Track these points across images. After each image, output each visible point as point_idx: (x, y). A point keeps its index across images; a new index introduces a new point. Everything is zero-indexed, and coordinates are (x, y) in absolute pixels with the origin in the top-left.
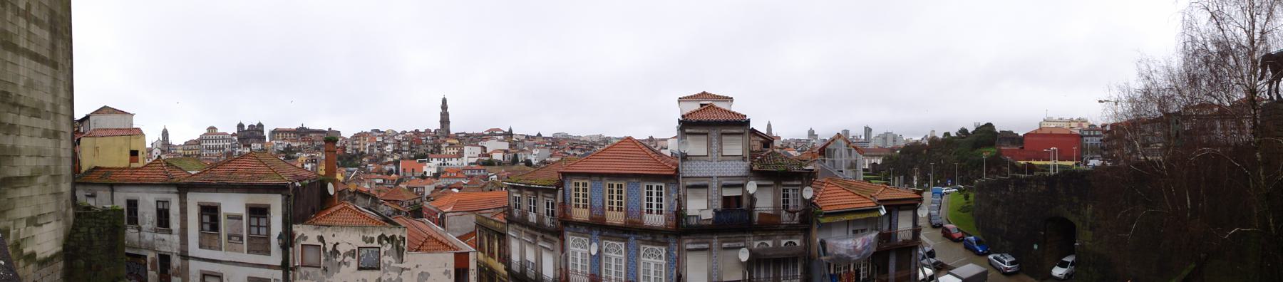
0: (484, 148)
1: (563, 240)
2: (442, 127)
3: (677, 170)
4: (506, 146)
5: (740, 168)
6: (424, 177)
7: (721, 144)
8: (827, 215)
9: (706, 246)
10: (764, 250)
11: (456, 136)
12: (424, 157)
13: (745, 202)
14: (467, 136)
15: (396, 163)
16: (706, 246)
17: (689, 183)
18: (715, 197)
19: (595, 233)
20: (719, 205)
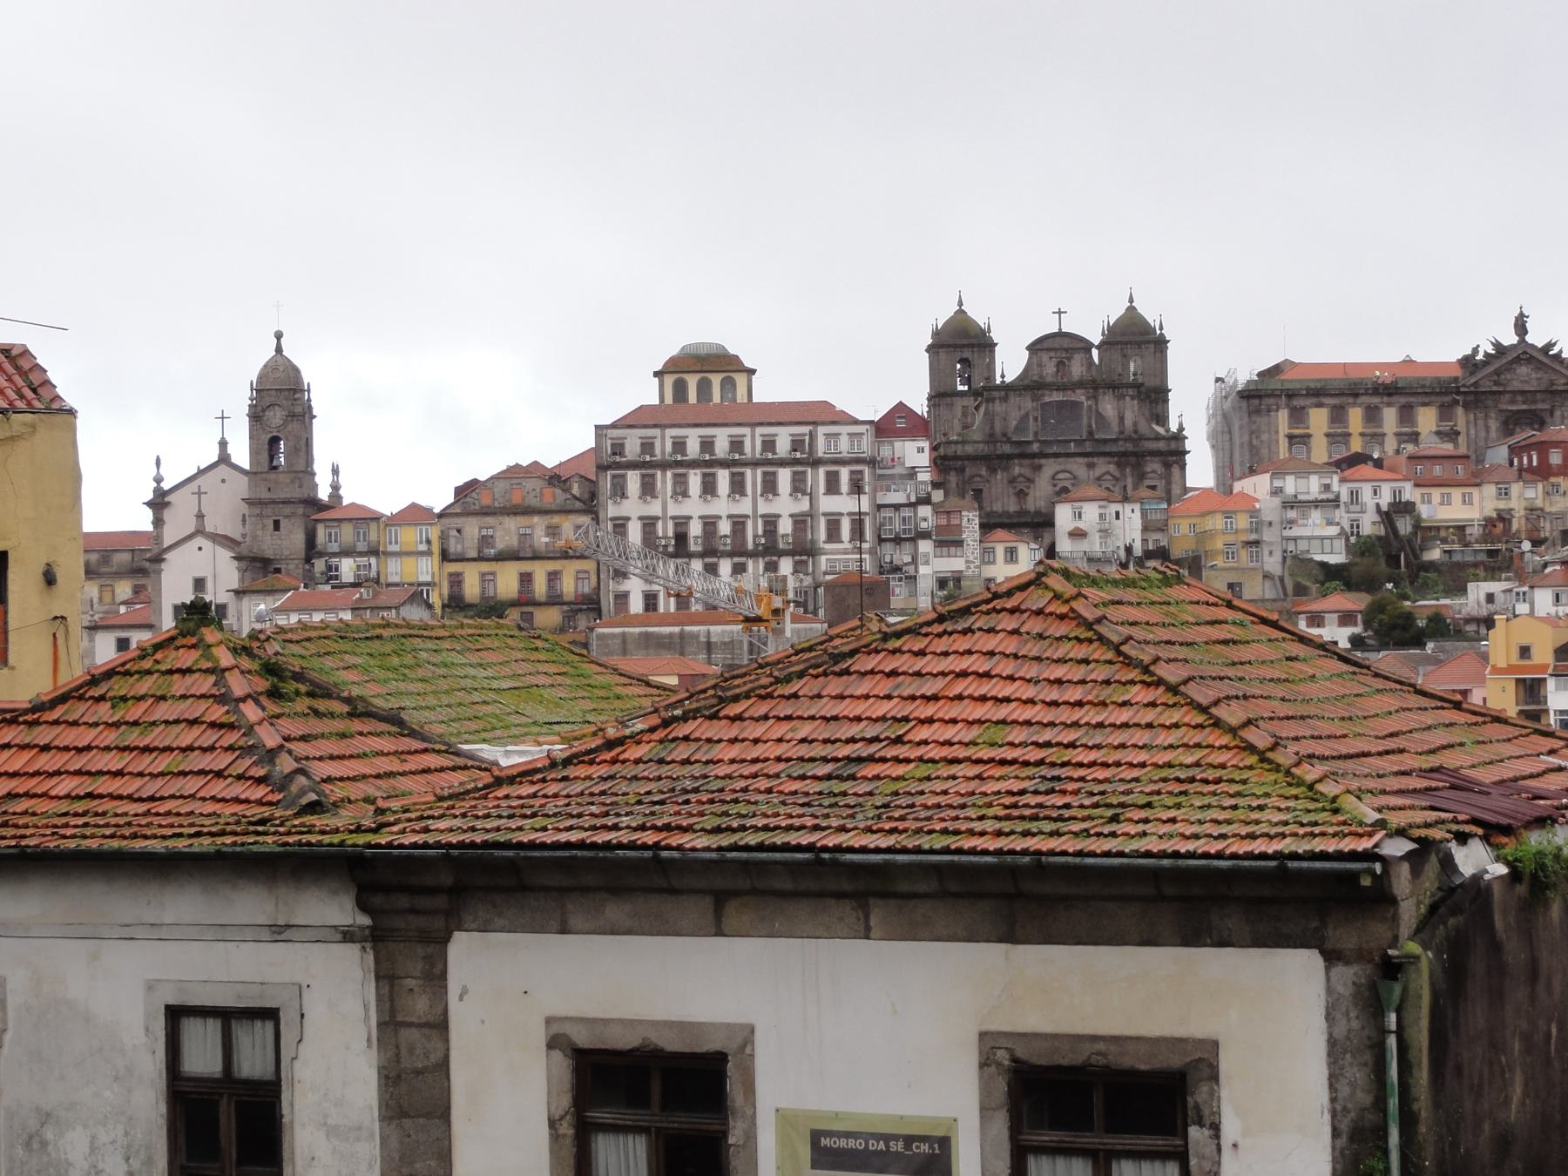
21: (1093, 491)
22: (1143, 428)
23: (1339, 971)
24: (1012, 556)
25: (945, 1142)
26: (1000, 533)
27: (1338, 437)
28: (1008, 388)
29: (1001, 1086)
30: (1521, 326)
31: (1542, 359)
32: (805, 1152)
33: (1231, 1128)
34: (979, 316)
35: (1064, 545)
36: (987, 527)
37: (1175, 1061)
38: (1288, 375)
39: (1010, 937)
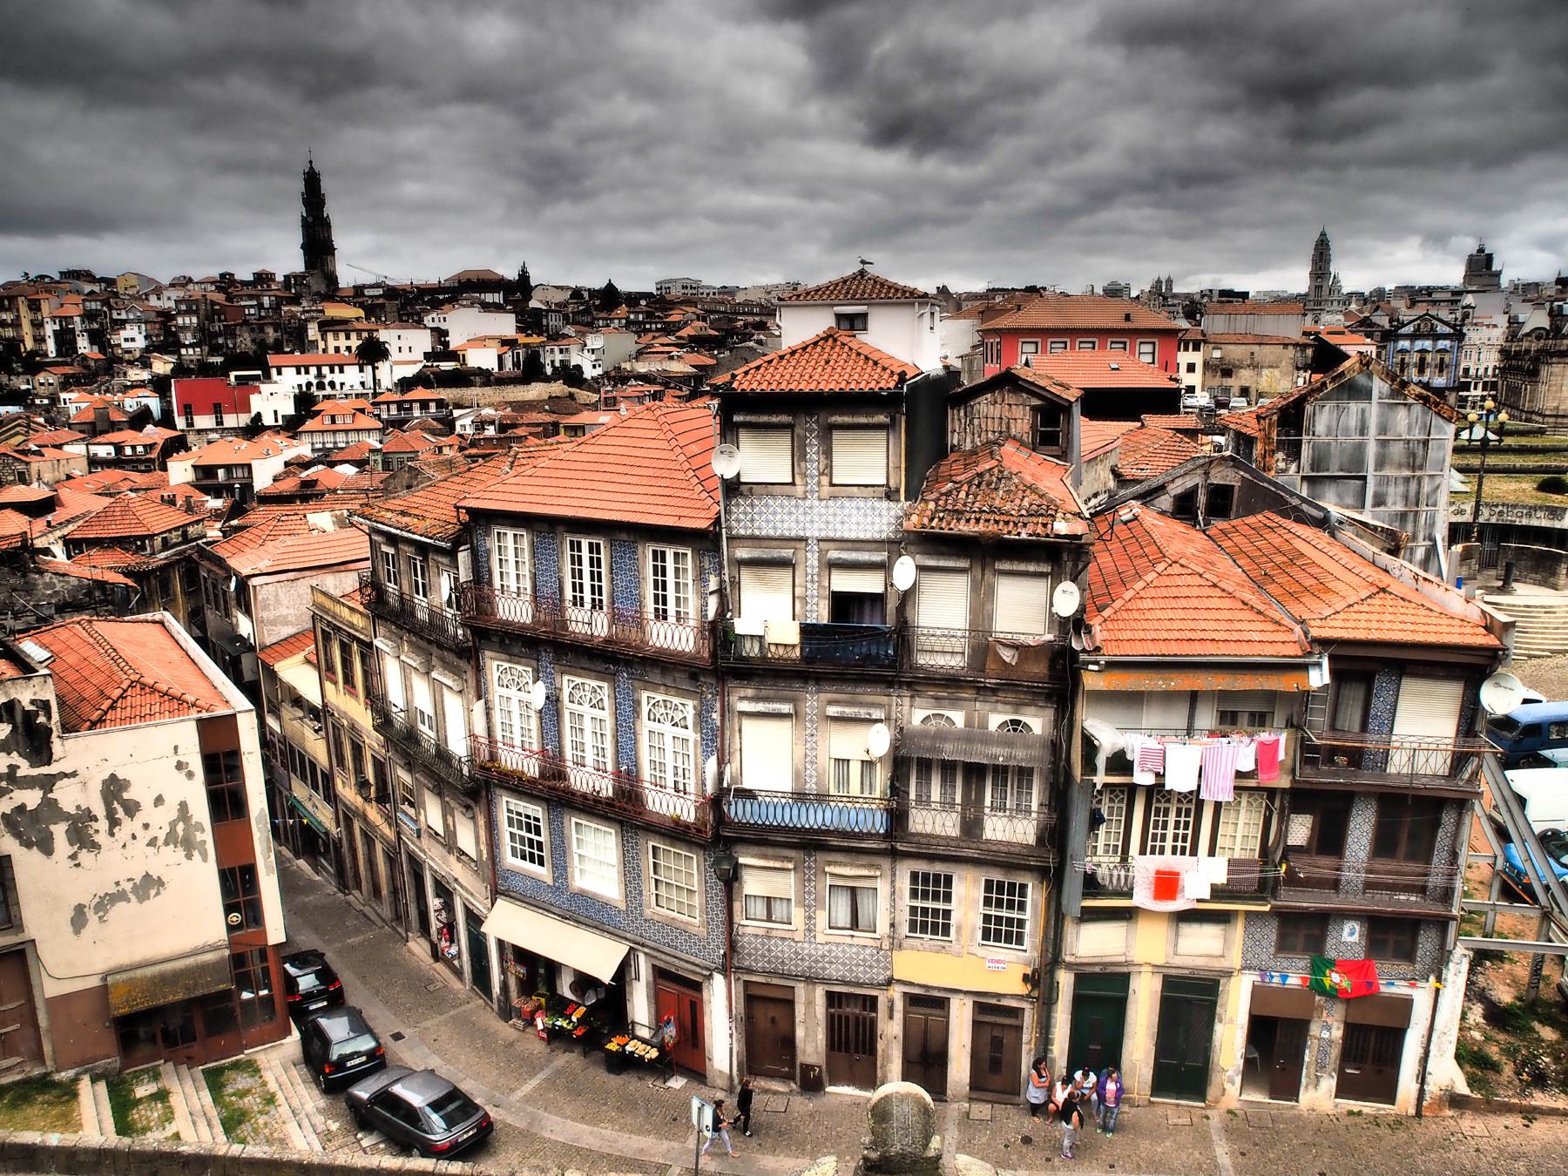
0: (440, 334)
1: (479, 670)
2: (309, 264)
3: (717, 521)
5: (879, 520)
6: (255, 429)
7: (828, 453)
8: (1112, 665)
9: (786, 708)
10: (940, 736)
12: (258, 363)
13: (892, 604)
14: (392, 293)
15: (160, 385)
16: (786, 708)
17: (742, 553)
18: (813, 589)
19: (546, 658)
20: (821, 613)
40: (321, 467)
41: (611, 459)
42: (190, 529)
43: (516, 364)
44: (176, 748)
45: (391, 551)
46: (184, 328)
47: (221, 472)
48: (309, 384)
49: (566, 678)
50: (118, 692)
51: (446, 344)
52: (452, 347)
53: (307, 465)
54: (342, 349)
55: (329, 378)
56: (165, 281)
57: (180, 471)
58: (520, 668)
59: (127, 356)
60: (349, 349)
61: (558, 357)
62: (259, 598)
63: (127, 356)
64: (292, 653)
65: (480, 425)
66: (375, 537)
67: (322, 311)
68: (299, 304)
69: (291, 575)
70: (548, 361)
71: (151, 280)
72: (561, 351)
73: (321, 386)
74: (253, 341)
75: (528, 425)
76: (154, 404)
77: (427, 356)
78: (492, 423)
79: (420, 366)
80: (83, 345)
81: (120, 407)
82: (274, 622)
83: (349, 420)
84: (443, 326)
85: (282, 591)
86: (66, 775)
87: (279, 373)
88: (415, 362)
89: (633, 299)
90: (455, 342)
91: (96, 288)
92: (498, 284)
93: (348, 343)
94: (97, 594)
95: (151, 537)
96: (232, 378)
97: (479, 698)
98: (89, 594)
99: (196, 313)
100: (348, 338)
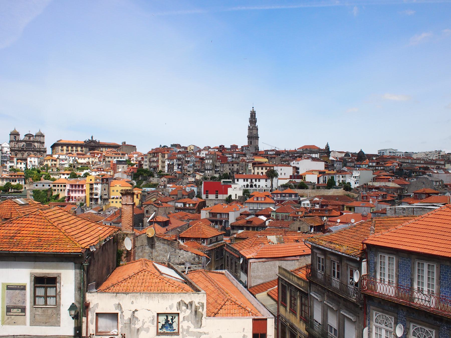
2: (250, 143)
4: (321, 166)
6: (229, 200)
11: (265, 154)
12: (231, 177)
14: (278, 153)
15: (197, 183)
21: (33, 155)
22: (41, 148)
23: (76, 265)
24: (21, 163)
25: (25, 286)
26: (19, 161)
27: (67, 150)
28: (21, 141)
29: (33, 278)
30: (92, 138)
31: (95, 142)
32: (6, 288)
33: (62, 284)
34: (18, 130)
35: (28, 163)
36: (17, 160)
37: (55, 276)
38: (61, 142)
39: (35, 262)
40: (253, 216)
41: (434, 228)
42: (219, 237)
43: (325, 181)
44: (244, 329)
45: (322, 257)
46: (208, 164)
47: (218, 215)
48: (247, 186)
49: (412, 325)
50: (224, 302)
51: (298, 172)
52: (300, 173)
53: (248, 215)
54: (260, 174)
55: (255, 183)
56: (202, 148)
57: (204, 214)
58: (387, 316)
59: (188, 173)
60: (262, 173)
61: (341, 179)
62: (252, 267)
63: (188, 173)
64: (263, 291)
65: (314, 203)
66: (315, 251)
67: (254, 159)
68: (245, 156)
69: (264, 260)
70: (337, 180)
71: (198, 148)
72: (343, 177)
73: (251, 186)
74: (230, 169)
75: (332, 205)
76: (195, 189)
77: (291, 177)
78: (318, 204)
79: (288, 181)
80: (175, 168)
81: (185, 190)
82: (255, 278)
83: (263, 200)
84: (297, 166)
85: (260, 265)
86: (205, 333)
87: (238, 181)
88: (286, 179)
89: (370, 157)
90: (301, 172)
91: (181, 150)
92: (319, 151)
93: (262, 171)
94: (197, 259)
95: (207, 239)
96: (222, 182)
97: (365, 327)
98: (194, 259)
99: (212, 159)
100: (262, 169)
